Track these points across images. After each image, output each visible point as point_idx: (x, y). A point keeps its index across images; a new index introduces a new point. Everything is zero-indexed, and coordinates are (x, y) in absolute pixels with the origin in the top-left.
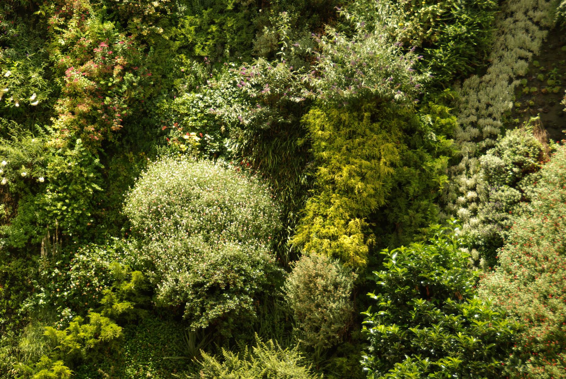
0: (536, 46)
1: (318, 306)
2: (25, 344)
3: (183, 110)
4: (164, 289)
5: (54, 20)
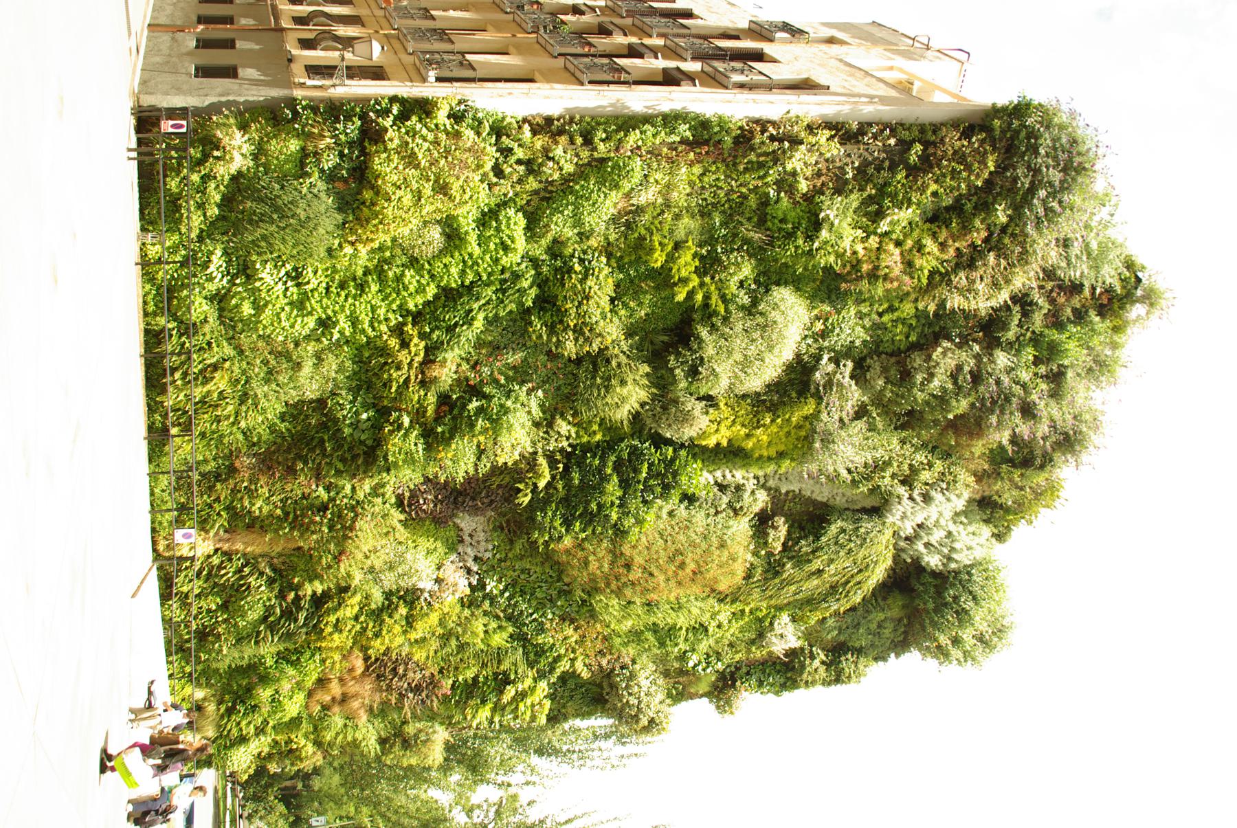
0: (819, 499)
1: (670, 425)
2: (686, 220)
3: (844, 313)
4: (704, 332)
5: (944, 234)
